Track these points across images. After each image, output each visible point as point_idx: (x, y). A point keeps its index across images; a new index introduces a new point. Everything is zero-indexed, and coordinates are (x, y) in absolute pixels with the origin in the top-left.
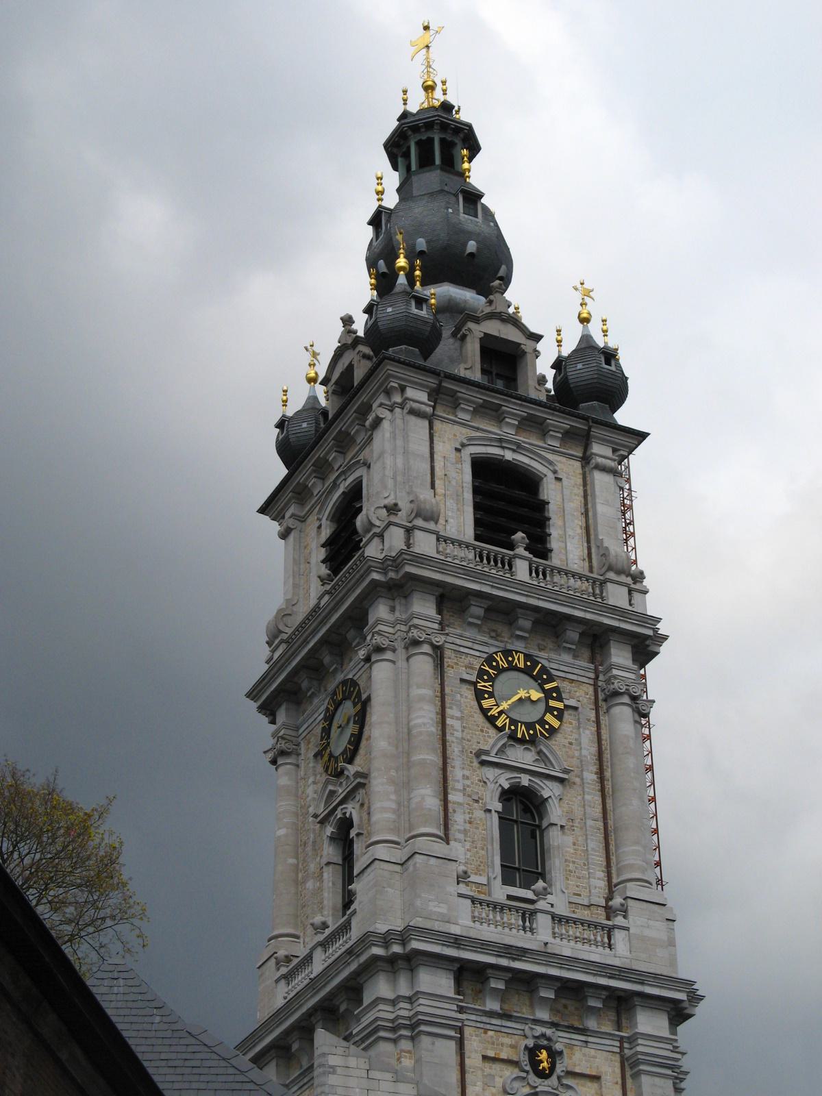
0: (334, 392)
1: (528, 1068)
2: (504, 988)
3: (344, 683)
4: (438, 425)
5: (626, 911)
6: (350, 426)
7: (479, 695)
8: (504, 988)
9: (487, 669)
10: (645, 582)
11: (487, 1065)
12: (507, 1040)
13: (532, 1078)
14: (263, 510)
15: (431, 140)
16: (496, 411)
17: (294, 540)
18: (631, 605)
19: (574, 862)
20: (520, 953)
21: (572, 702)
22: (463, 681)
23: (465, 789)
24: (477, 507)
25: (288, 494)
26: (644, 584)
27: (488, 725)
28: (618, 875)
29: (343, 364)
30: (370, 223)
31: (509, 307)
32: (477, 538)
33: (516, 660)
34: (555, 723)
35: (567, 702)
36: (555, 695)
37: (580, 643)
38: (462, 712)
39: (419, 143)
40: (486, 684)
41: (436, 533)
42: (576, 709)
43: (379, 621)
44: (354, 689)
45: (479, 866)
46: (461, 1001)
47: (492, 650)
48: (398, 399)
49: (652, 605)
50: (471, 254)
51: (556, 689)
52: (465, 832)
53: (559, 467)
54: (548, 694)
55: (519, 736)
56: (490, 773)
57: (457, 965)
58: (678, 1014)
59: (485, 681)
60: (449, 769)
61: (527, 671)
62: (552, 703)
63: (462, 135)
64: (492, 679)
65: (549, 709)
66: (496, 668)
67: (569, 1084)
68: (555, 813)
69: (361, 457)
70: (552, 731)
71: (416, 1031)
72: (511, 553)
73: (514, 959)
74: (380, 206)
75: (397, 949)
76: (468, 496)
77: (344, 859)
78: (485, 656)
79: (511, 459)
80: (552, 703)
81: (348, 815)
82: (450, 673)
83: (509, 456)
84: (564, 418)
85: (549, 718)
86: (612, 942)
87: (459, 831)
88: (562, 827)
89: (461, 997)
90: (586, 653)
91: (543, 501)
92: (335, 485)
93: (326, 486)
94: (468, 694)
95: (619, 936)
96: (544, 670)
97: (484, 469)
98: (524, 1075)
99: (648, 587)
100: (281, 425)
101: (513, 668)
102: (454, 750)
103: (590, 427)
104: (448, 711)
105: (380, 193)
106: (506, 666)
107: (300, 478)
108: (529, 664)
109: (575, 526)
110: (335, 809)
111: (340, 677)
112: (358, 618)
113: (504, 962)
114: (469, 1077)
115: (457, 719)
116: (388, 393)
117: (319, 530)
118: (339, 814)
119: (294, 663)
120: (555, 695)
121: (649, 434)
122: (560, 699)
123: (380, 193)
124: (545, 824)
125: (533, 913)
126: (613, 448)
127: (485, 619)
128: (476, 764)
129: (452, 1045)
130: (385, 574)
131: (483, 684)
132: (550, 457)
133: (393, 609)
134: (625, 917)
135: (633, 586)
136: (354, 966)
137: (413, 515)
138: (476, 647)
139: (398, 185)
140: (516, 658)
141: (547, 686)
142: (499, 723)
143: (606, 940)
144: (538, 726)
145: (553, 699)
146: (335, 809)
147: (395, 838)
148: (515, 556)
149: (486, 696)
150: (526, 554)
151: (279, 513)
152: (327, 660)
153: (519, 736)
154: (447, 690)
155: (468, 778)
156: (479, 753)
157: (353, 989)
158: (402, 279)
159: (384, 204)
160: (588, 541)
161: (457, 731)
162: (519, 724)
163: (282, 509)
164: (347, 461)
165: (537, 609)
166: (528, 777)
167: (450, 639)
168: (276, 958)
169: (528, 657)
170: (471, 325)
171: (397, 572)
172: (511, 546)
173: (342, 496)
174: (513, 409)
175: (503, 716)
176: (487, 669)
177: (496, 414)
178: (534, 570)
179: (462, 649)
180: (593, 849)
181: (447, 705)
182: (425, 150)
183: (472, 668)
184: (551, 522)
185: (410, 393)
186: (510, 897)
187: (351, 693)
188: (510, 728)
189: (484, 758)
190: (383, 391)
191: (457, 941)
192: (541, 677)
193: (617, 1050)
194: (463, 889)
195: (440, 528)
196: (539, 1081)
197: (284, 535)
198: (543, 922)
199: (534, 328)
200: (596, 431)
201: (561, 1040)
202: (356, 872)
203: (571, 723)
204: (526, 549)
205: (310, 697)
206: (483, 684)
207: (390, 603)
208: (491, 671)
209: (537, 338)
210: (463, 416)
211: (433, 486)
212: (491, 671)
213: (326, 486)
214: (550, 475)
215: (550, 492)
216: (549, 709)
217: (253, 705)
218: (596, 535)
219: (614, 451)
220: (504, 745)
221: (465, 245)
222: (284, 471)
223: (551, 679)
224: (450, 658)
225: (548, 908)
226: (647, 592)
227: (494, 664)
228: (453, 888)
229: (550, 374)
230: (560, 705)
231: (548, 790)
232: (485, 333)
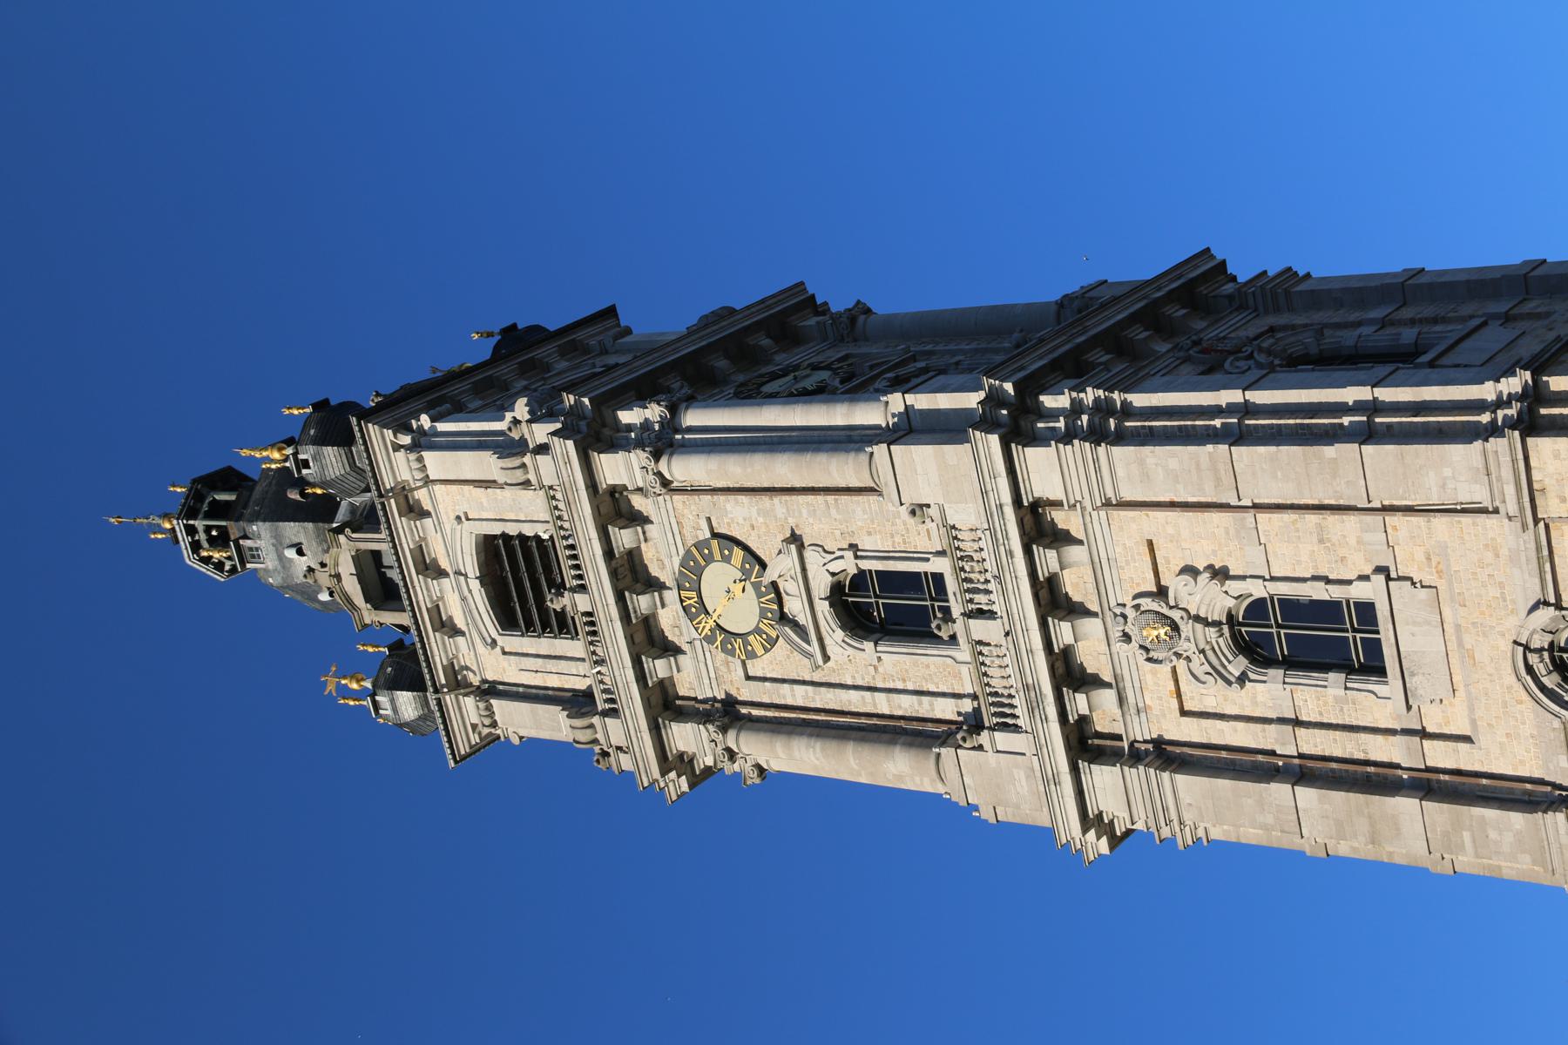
9: (718, 643)
19: (892, 536)
33: (691, 602)
35: (708, 535)
45: (949, 673)
87: (920, 703)
131: (738, 650)
140: (689, 602)
144: (753, 580)
162: (762, 605)
176: (718, 643)
179: (712, 675)
180: (864, 512)
206: (738, 650)
208: (719, 639)
212: (719, 639)
231: (821, 584)
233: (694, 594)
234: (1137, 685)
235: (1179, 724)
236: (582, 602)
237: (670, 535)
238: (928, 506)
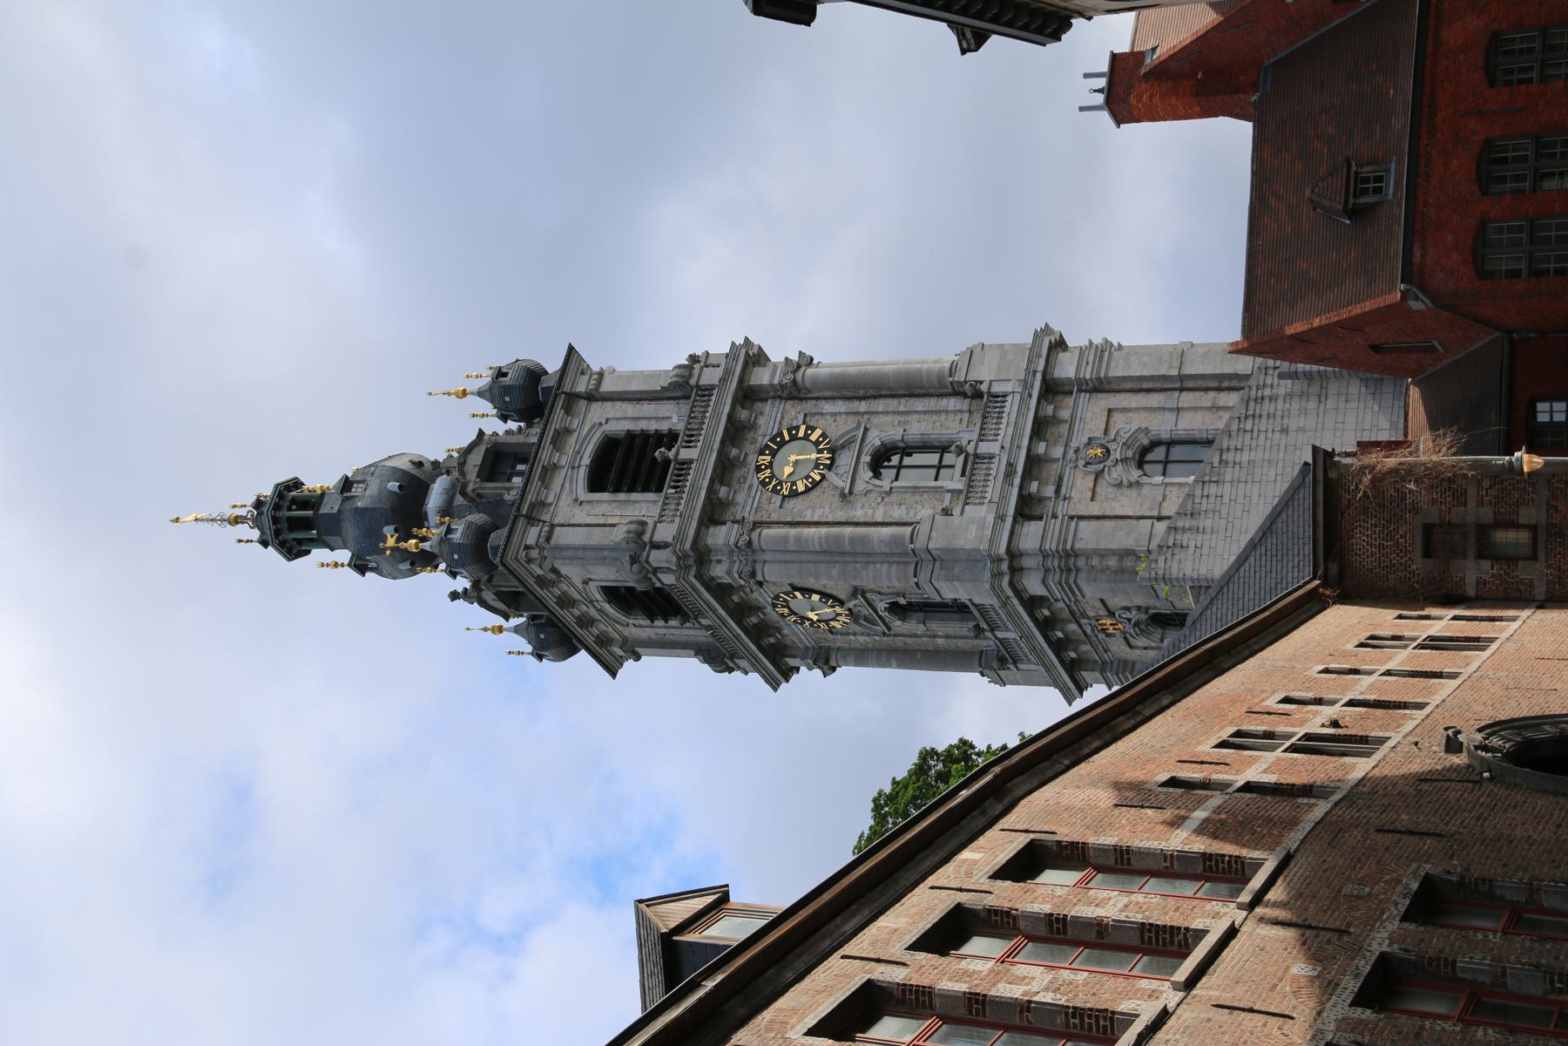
0: (517, 609)
1: (1101, 466)
2: (1037, 482)
3: (774, 606)
4: (556, 521)
5: (976, 382)
6: (553, 595)
7: (794, 494)
8: (1037, 482)
9: (771, 486)
11: (1098, 497)
12: (1079, 482)
13: (1108, 463)
14: (614, 675)
15: (290, 519)
18: (718, 366)
20: (1011, 466)
21: (801, 418)
22: (781, 507)
23: (873, 508)
24: (631, 490)
25: (602, 652)
26: (700, 354)
27: (818, 488)
28: (946, 387)
30: (364, 575)
31: (452, 456)
32: (659, 490)
33: (765, 462)
34: (818, 432)
35: (801, 422)
36: (794, 432)
37: (750, 409)
38: (808, 508)
39: (291, 530)
40: (785, 487)
41: (656, 523)
42: (805, 415)
43: (729, 573)
44: (782, 597)
46: (1047, 516)
47: (756, 482)
49: (720, 347)
50: (400, 487)
51: (789, 431)
52: (909, 509)
53: (596, 420)
54: (794, 438)
55: (828, 462)
56: (860, 486)
57: (1019, 519)
58: (1060, 345)
59: (782, 488)
60: (855, 520)
61: (774, 454)
62: (801, 434)
63: (285, 492)
64: (780, 483)
65: (806, 437)
66: (771, 478)
67: (1115, 432)
68: (894, 434)
69: (580, 586)
70: (824, 435)
71: (1071, 552)
73: (1015, 472)
74: (349, 565)
75: (1005, 566)
76: (622, 496)
77: (921, 611)
78: (760, 487)
79: (589, 460)
80: (801, 434)
81: (887, 606)
82: (774, 517)
83: (586, 461)
84: (555, 414)
85: (813, 437)
86: (1001, 394)
88: (905, 431)
89: (1045, 516)
90: (759, 405)
91: (626, 435)
92: (600, 611)
93: (600, 618)
94: (791, 504)
95: (996, 389)
96: (773, 440)
97: (597, 482)
98: (1106, 469)
100: (540, 658)
101: (771, 464)
102: (841, 515)
103: (563, 393)
104: (807, 519)
105: (336, 565)
106: (769, 471)
107: (590, 640)
108: (767, 452)
109: (647, 409)
110: (880, 617)
111: (769, 609)
112: (721, 591)
113: (1017, 481)
114: (1108, 513)
115: (814, 511)
116: (529, 561)
117: (638, 627)
118: (885, 614)
119: (754, 648)
120: (794, 432)
122: (797, 428)
123: (336, 565)
124: (901, 445)
125: (976, 456)
127: (729, 485)
128: (852, 498)
129: (1083, 524)
130: (690, 566)
131: (784, 490)
132: (587, 428)
133: (719, 561)
134: (981, 383)
135: (702, 364)
136: (1015, 601)
138: (753, 494)
139: (328, 550)
140: (762, 462)
141: (787, 438)
142: (818, 478)
143: (1000, 399)
144: (821, 447)
145: (797, 433)
146: (880, 617)
147: (913, 565)
148: (676, 459)
149: (794, 488)
150: (674, 450)
151: (617, 660)
152: (754, 620)
153: (828, 462)
154: (789, 519)
155: (863, 505)
156: (843, 496)
157: (1032, 604)
159: (346, 562)
160: (662, 399)
161: (824, 513)
163: (614, 657)
164: (582, 599)
165: (723, 442)
166: (863, 456)
168: (999, 669)
169: (762, 453)
170: (470, 488)
172: (667, 462)
174: (546, 455)
175: (812, 474)
176: (771, 486)
177: (550, 470)
178: (689, 444)
179: (755, 506)
181: (802, 520)
182: (296, 524)
183: (771, 499)
184: (645, 429)
186: (963, 474)
187: (785, 600)
188: (822, 470)
189: (847, 491)
191: (1001, 518)
192: (778, 443)
193: (1088, 395)
194: (956, 512)
195: (650, 522)
196: (1112, 457)
197: (638, 657)
198: (984, 448)
199: (473, 437)
200: (567, 388)
201: (1079, 440)
202: (938, 599)
203: (818, 420)
204: (670, 450)
205: (782, 636)
207: (714, 564)
208: (773, 483)
209: (481, 433)
210: (550, 500)
211: (613, 525)
212: (773, 483)
213: (600, 618)
215: (619, 427)
216: (806, 437)
217: (784, 685)
218: (656, 391)
219: (583, 373)
220: (836, 474)
221: (391, 492)
222: (583, 654)
223: (780, 434)
224: (762, 517)
225: (972, 444)
226: (707, 352)
227: (767, 480)
228: (956, 519)
229: (513, 425)
230: (803, 428)
232: (477, 477)
233: (769, 458)
234: (1070, 484)
235: (1087, 506)
236: (685, 454)
237: (772, 423)
238: (981, 383)
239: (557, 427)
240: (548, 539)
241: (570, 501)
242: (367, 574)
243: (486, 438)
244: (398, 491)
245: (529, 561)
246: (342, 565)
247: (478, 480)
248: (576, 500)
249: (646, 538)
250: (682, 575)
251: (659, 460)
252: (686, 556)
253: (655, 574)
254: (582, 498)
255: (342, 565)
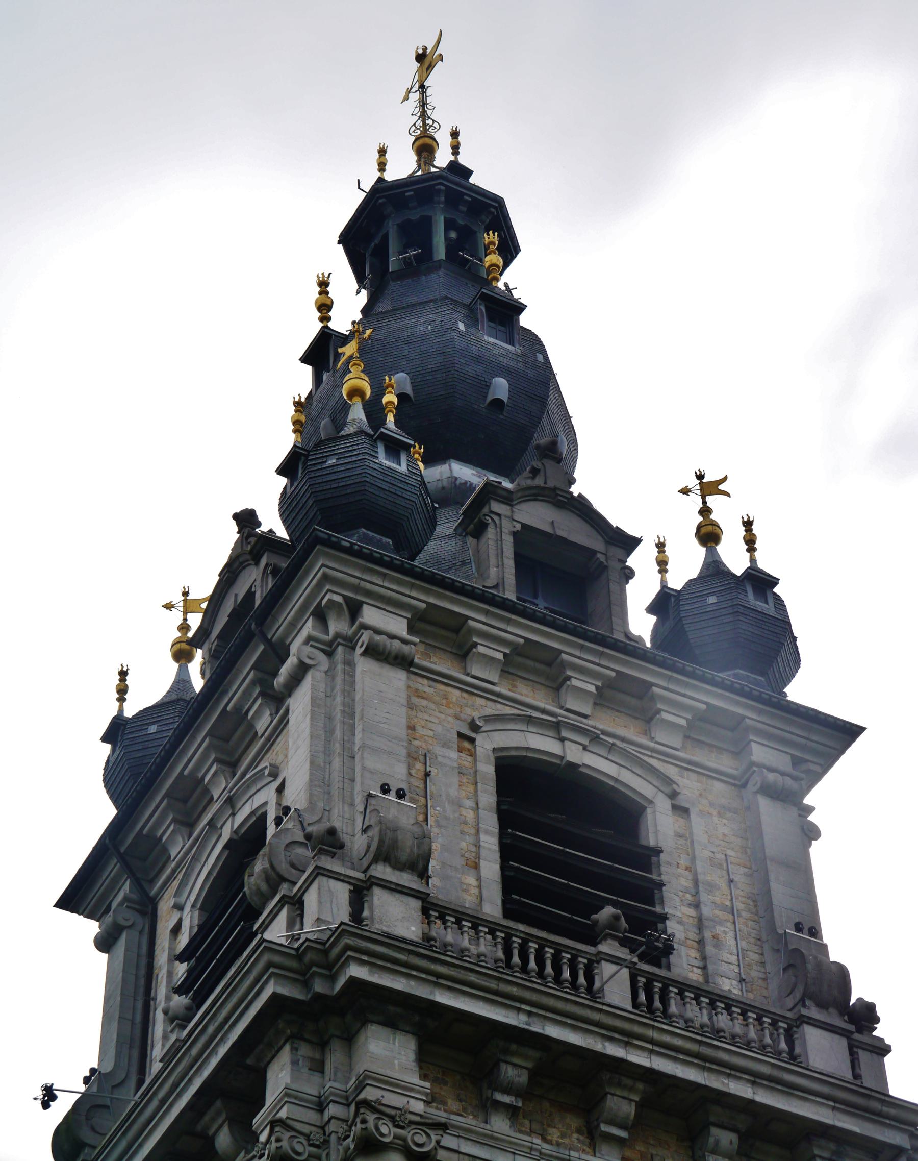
10: (880, 1031)
16: (549, 664)
17: (127, 950)
24: (507, 852)
29: (236, 595)
30: (305, 359)
48: (337, 626)
50: (498, 403)
72: (591, 949)
83: (574, 754)
99: (887, 1042)
121: (863, 729)
126: (792, 756)
130: (306, 984)
135: (857, 1036)
137: (370, 856)
150: (623, 953)
158: (357, 413)
167: (449, 1141)
170: (496, 507)
171: (333, 978)
173: (227, 853)
185: (371, 615)
190: (313, 614)
209: (631, 543)
214: (662, 804)
219: (796, 762)
221: (487, 386)
232: (524, 526)
239: (655, 689)
240: (373, 652)
241: (470, 713)
242: (308, 370)
243: (618, 552)
244: (490, 398)
245: (321, 616)
246: (325, 319)
247: (518, 527)
248: (475, 727)
249: (382, 871)
250: (277, 959)
251: (594, 916)
252: (331, 969)
253: (284, 901)
254: (480, 739)
255: (325, 319)
